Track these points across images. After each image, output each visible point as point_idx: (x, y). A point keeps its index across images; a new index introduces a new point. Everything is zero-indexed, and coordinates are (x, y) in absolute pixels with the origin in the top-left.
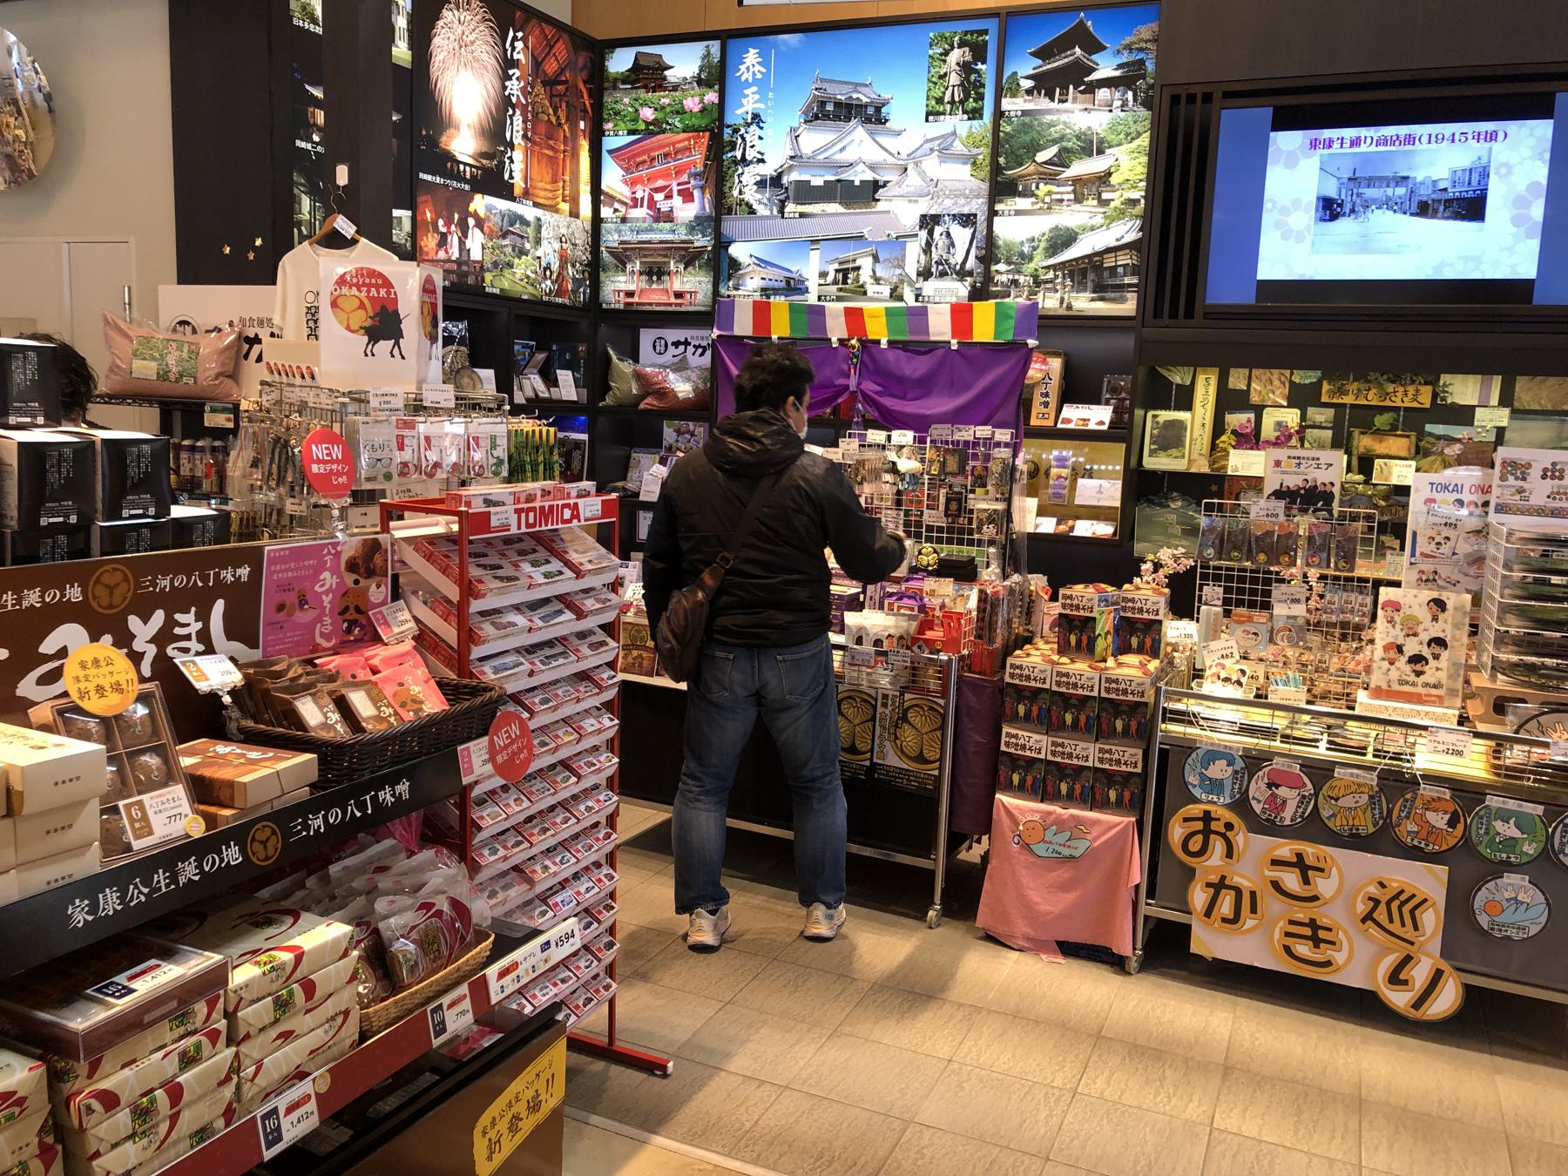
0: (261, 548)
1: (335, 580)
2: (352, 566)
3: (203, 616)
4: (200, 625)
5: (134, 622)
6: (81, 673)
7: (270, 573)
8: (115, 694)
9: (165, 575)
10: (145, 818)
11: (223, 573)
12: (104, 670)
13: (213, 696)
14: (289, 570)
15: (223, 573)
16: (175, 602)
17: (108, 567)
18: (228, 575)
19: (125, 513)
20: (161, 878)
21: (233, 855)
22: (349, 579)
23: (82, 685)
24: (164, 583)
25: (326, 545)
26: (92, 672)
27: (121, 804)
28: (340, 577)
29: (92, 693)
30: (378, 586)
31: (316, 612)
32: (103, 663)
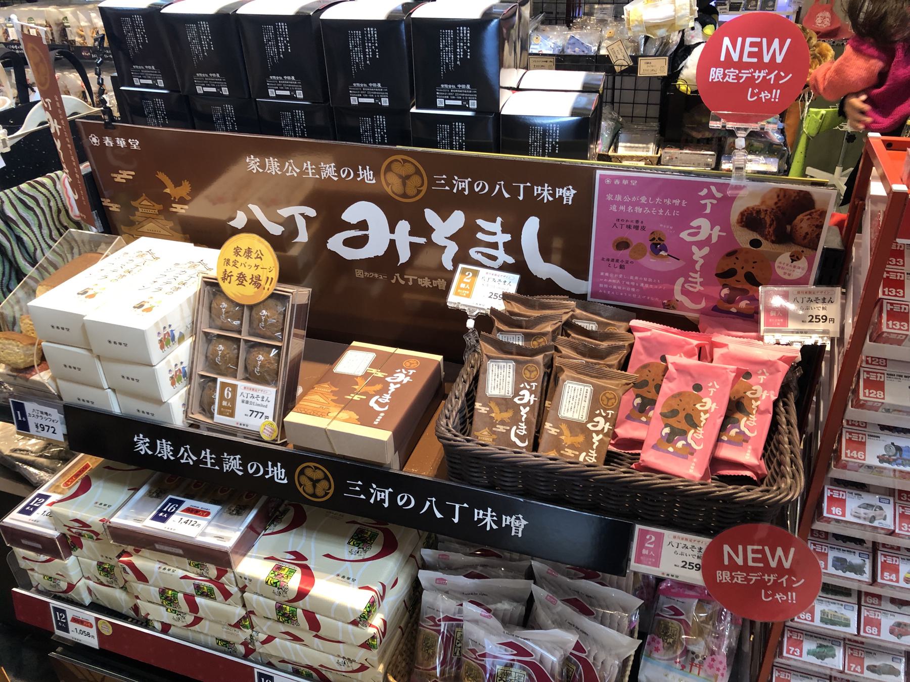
0: (592, 171)
1: (716, 232)
2: (750, 220)
3: (514, 228)
4: (508, 237)
5: (431, 216)
6: (233, 258)
7: (603, 203)
8: (252, 286)
9: (463, 176)
10: (233, 400)
11: (537, 190)
12: (252, 261)
13: (461, 315)
14: (638, 204)
15: (537, 190)
16: (476, 206)
17: (399, 157)
18: (544, 193)
19: (440, 102)
20: (207, 454)
21: (278, 474)
22: (744, 237)
23: (229, 269)
24: (463, 185)
25: (707, 185)
26: (242, 259)
27: (220, 379)
28: (726, 227)
29: (234, 278)
30: (795, 258)
31: (681, 263)
32: (254, 255)
